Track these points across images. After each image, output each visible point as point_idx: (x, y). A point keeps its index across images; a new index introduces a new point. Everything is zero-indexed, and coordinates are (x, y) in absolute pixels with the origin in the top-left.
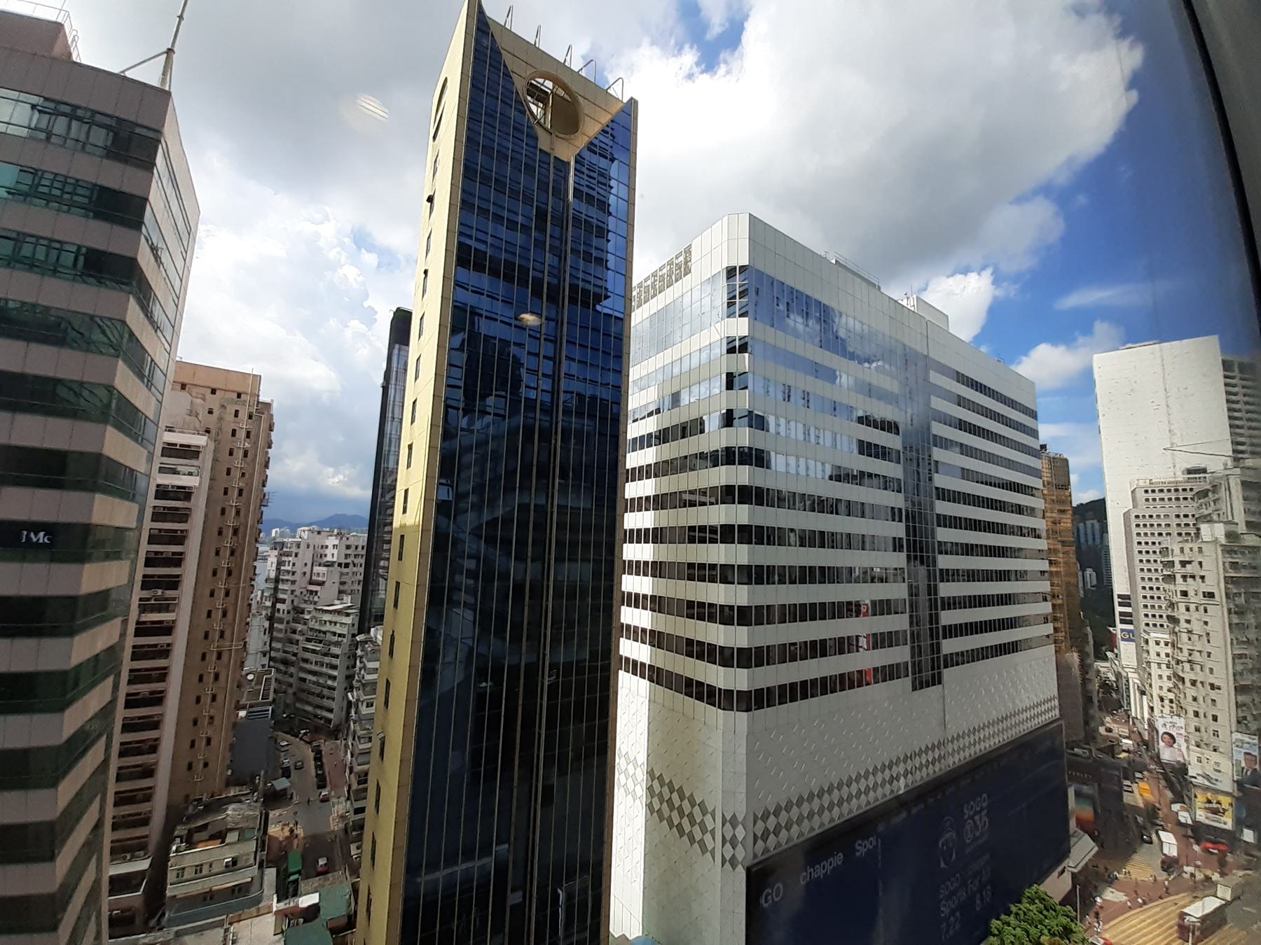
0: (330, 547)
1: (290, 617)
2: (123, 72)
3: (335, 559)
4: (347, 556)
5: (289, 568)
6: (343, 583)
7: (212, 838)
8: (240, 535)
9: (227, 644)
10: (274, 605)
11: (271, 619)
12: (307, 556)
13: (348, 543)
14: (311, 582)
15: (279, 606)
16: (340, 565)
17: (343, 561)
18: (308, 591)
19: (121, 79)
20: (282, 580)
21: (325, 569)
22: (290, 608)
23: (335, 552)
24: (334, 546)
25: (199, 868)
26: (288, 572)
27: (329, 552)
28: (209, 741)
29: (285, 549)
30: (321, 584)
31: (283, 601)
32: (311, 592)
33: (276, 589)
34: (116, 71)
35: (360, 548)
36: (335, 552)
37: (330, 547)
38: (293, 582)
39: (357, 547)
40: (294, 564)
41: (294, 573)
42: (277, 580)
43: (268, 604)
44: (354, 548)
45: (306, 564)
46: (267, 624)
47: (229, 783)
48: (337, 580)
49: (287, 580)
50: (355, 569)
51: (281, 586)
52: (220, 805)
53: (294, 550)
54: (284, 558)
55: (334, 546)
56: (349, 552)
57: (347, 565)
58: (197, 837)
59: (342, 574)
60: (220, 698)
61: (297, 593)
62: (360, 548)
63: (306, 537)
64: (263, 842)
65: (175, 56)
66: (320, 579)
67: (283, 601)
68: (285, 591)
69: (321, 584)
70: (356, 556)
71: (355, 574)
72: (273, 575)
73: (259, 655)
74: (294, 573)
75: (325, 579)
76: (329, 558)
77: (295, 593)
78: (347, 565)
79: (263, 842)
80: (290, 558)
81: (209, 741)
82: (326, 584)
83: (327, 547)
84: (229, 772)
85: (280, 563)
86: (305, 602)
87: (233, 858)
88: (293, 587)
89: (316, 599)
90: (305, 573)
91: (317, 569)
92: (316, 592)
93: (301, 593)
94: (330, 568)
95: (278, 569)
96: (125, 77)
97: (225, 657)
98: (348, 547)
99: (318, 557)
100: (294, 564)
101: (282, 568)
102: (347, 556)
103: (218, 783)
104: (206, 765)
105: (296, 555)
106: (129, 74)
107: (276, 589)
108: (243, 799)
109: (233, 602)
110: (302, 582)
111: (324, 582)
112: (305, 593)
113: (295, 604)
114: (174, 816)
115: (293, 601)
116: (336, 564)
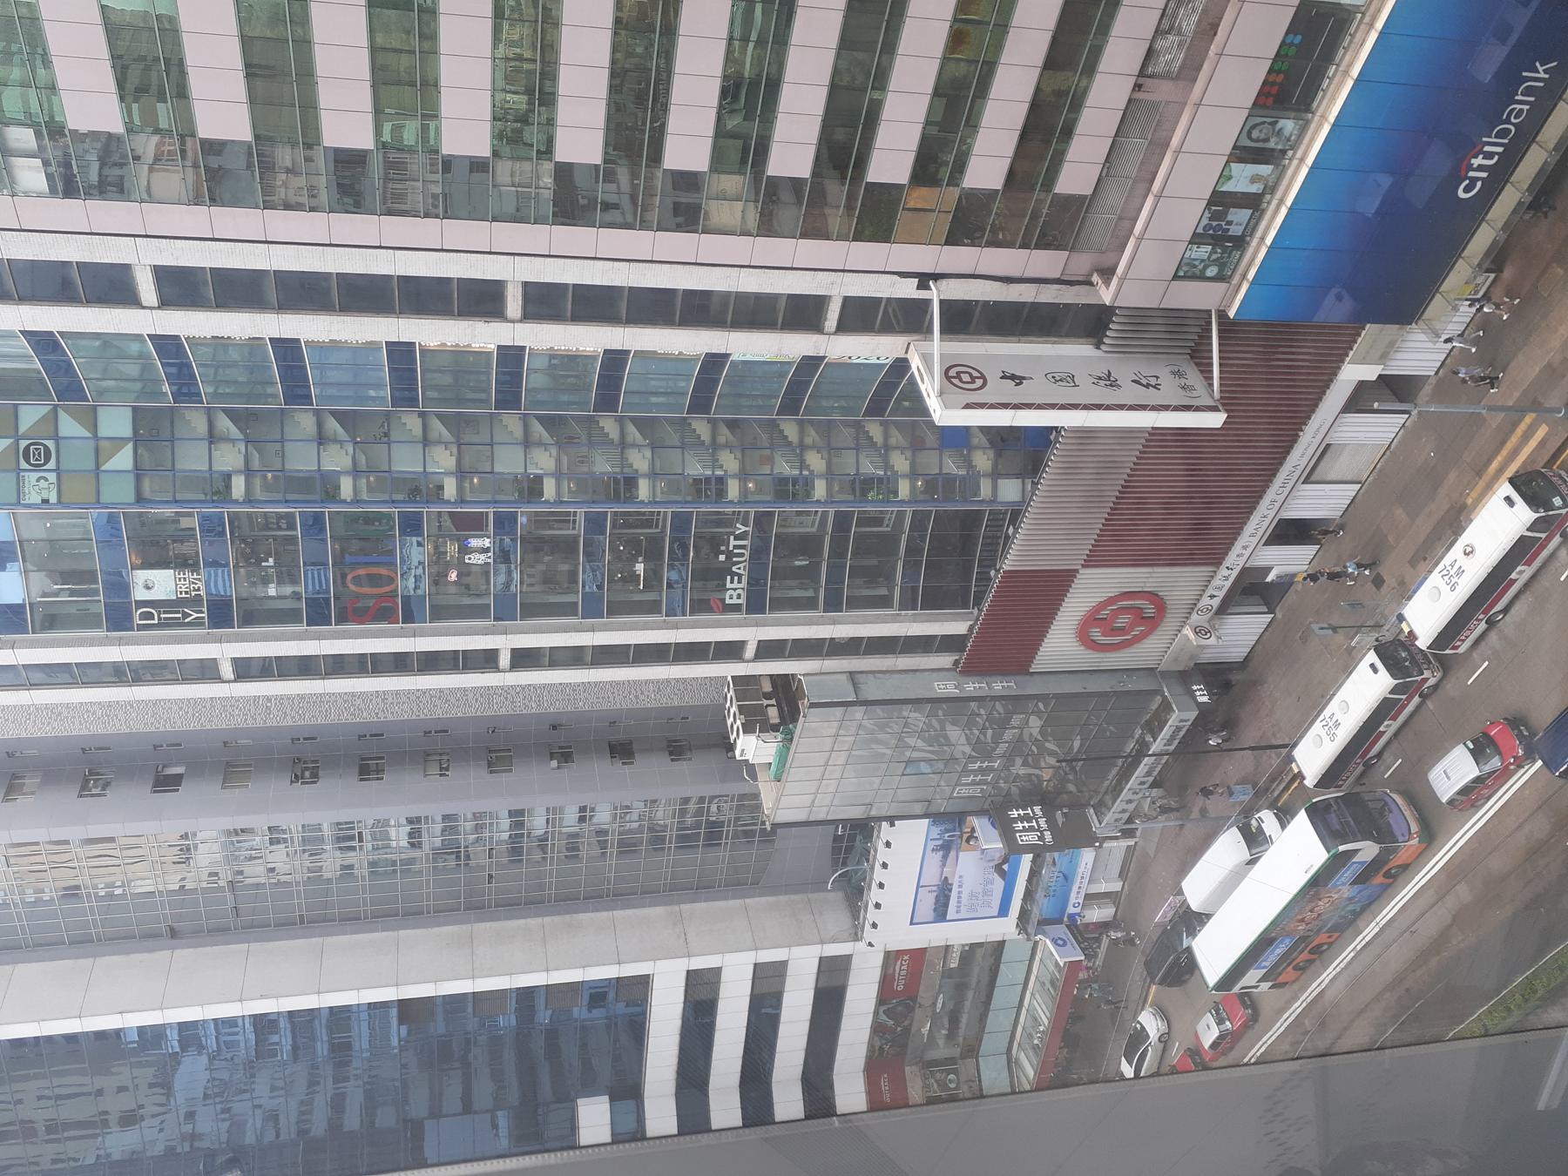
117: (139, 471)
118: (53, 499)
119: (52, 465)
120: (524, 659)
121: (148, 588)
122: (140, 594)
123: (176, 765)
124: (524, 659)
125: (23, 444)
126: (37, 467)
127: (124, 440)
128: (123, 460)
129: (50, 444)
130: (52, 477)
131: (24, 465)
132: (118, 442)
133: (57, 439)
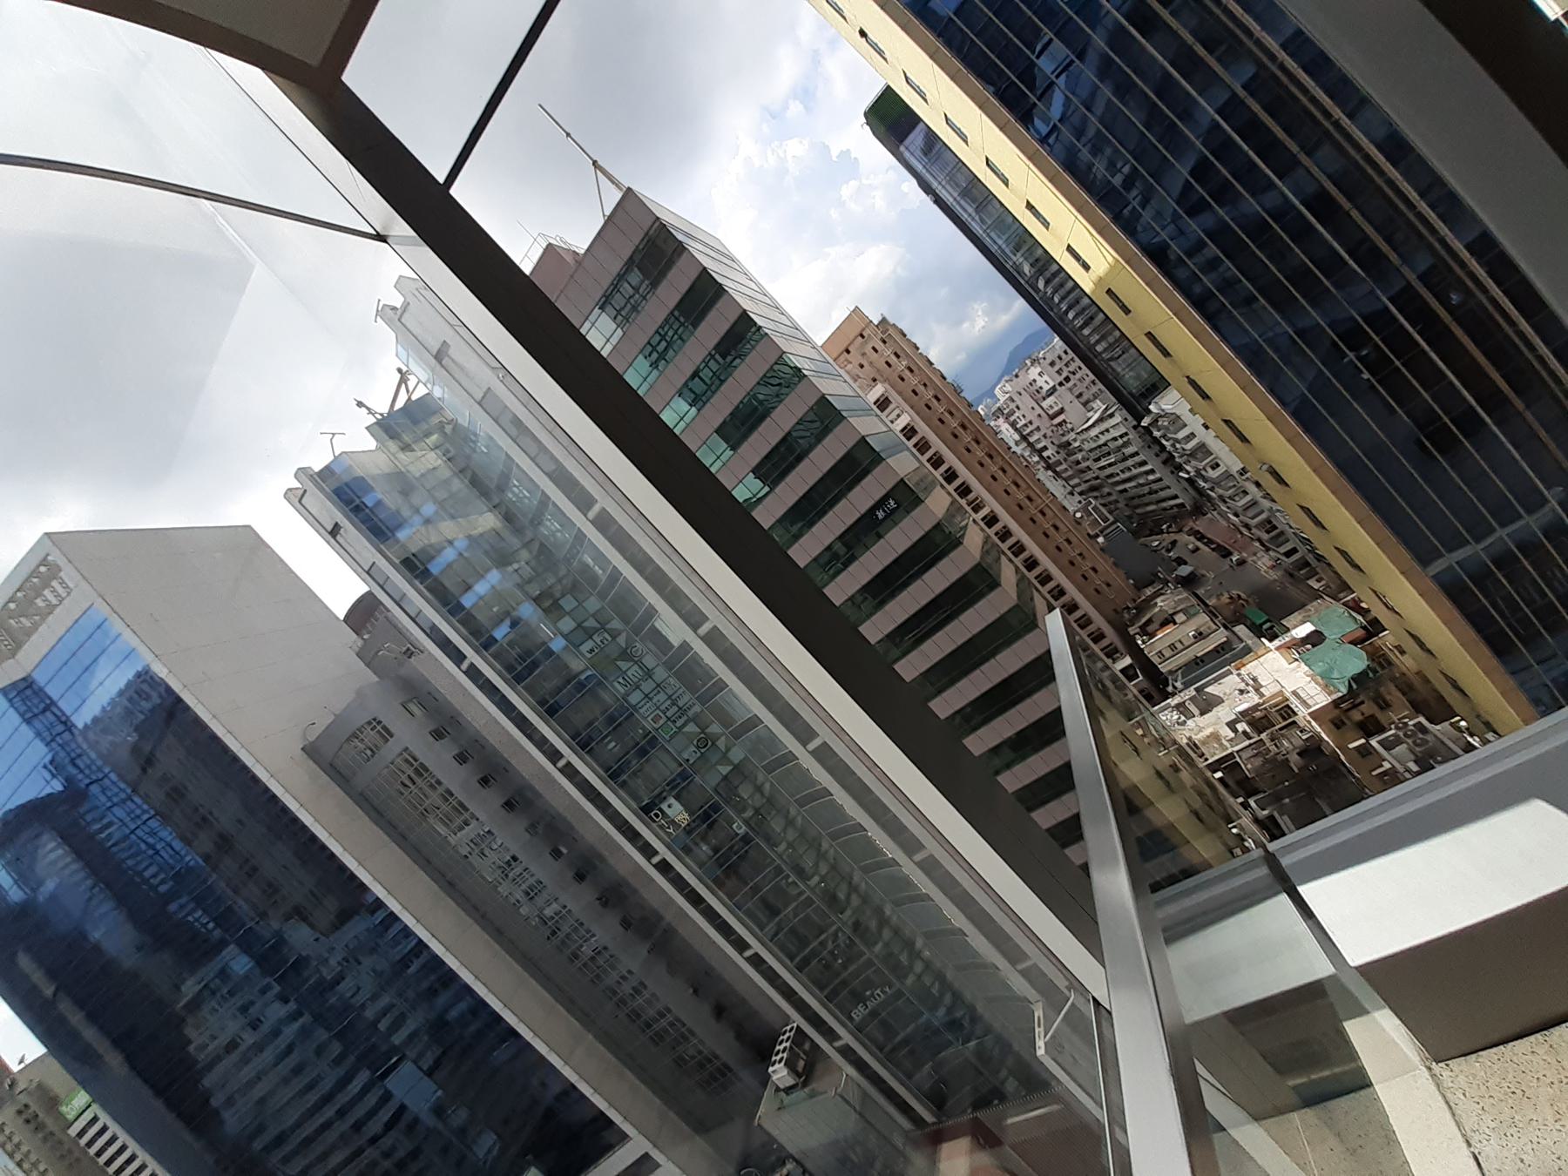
0: (1038, 378)
1: (1063, 454)
2: (604, 216)
3: (1052, 384)
4: (1059, 372)
5: (1023, 422)
6: (1080, 395)
7: (1164, 624)
8: (968, 425)
9: (1040, 501)
10: (1041, 457)
11: (1049, 467)
12: (1026, 402)
13: (1048, 361)
14: (1052, 417)
15: (1045, 454)
16: (1061, 384)
17: (1061, 379)
18: (1056, 426)
19: (610, 220)
20: (1028, 435)
21: (1052, 398)
22: (1056, 448)
23: (1046, 377)
24: (1039, 374)
25: (1172, 647)
26: (1026, 425)
27: (1040, 382)
28: (1094, 569)
29: (1005, 412)
30: (1062, 411)
31: (1045, 448)
32: (1060, 424)
33: (1030, 445)
34: (602, 222)
35: (1064, 356)
36: (1046, 377)
37: (1038, 378)
38: (1038, 429)
39: (1060, 358)
40: (1024, 416)
41: (1031, 423)
42: (1024, 438)
43: (1036, 459)
44: (1058, 361)
45: (1033, 408)
46: (1050, 473)
47: (1139, 587)
48: (1071, 397)
49: (1032, 432)
50: (1078, 376)
51: (1032, 440)
52: (1149, 603)
53: (1012, 406)
54: (1012, 419)
55: (1039, 374)
56: (1057, 368)
57: (1067, 379)
58: (1150, 629)
59: (1070, 390)
60: (1073, 539)
61: (1049, 433)
62: (1064, 356)
63: (1010, 389)
64: (1211, 612)
65: (600, 163)
66: (1056, 409)
67: (1045, 448)
68: (1038, 441)
69: (1062, 411)
70: (1066, 365)
71: (1081, 380)
72: (1017, 437)
73: (1068, 497)
74: (1031, 423)
75: (1060, 406)
76: (1046, 388)
77: (1048, 435)
78: (1067, 379)
79: (1211, 612)
80: (1017, 414)
81: (1094, 569)
82: (1066, 408)
83: (1035, 381)
84: (1132, 581)
85: (1013, 425)
86: (1063, 435)
87: (1195, 631)
88: (1042, 433)
89: (1069, 426)
90: (1039, 415)
91: (1045, 404)
92: (1064, 421)
93: (1053, 431)
94: (1056, 394)
95: (1016, 430)
96: (609, 217)
97: (1047, 511)
98: (1052, 364)
99: (1038, 395)
100: (1024, 416)
101: (1018, 426)
102: (1059, 372)
103: (1131, 593)
104: (1108, 585)
105: (1018, 408)
106: (608, 213)
107: (1030, 445)
108: (1163, 591)
109: (1013, 472)
110: (1045, 424)
111: (1062, 409)
112: (1055, 429)
113: (1056, 442)
114: (1122, 630)
115: (1052, 442)
116: (1057, 387)
117: (725, 778)
118: (691, 762)
119: (703, 750)
120: (756, 961)
121: (669, 806)
122: (664, 806)
123: (567, 848)
124: (756, 961)
125: (702, 735)
126: (698, 747)
127: (732, 763)
128: (725, 770)
129: (710, 743)
130: (699, 754)
131: (695, 742)
132: (730, 762)
133: (713, 743)
